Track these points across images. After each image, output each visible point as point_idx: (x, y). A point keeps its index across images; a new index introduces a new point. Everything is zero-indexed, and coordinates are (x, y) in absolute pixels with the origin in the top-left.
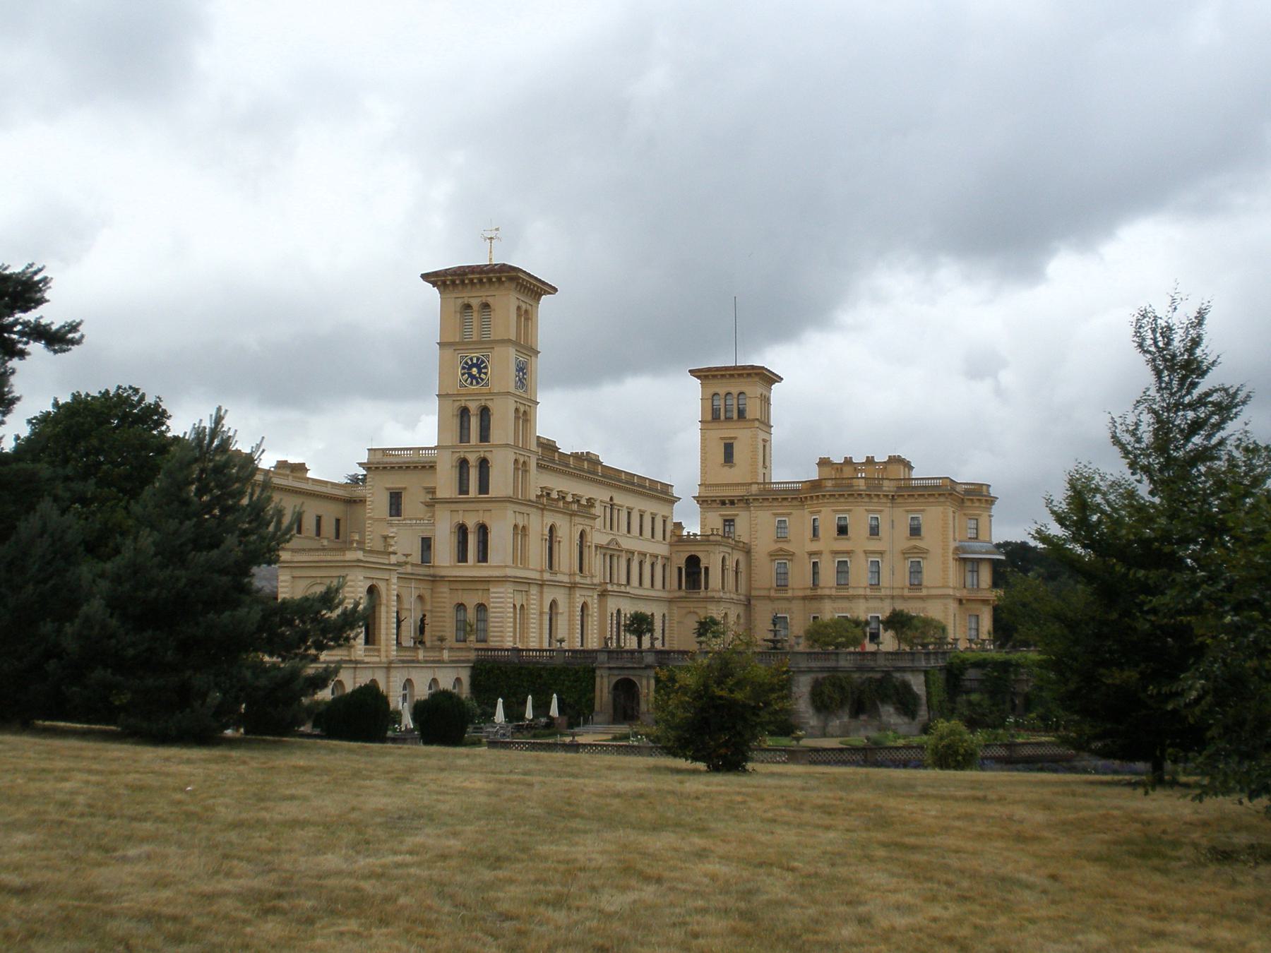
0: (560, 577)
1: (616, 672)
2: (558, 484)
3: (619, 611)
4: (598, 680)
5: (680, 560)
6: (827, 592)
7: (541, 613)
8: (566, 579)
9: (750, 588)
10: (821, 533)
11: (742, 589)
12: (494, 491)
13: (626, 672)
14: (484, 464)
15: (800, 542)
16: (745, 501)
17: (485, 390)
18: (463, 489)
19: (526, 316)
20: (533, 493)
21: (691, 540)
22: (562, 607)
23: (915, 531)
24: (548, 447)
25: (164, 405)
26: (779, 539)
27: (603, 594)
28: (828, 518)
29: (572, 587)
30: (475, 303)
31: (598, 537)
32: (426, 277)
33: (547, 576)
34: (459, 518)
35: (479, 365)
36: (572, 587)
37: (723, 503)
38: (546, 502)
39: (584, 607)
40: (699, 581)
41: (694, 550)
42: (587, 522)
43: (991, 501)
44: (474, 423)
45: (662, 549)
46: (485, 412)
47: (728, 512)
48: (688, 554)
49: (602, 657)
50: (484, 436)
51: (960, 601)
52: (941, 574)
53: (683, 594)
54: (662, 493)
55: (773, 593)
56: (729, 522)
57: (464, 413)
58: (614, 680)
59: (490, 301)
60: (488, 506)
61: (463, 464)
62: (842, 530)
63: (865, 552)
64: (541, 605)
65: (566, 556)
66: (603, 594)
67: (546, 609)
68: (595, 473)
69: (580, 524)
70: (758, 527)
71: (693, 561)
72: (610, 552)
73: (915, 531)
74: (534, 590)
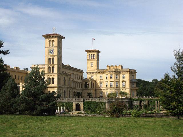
0: (66, 86)
1: (77, 102)
2: (65, 70)
3: (74, 92)
5: (84, 83)
6: (108, 88)
7: (63, 93)
8: (66, 87)
9: (96, 88)
10: (108, 78)
11: (95, 88)
12: (55, 72)
14: (53, 67)
15: (104, 80)
17: (53, 55)
18: (49, 72)
19: (60, 43)
20: (61, 72)
21: (86, 79)
22: (66, 91)
23: (124, 77)
24: (63, 64)
25: (2, 59)
26: (100, 79)
27: (72, 89)
28: (109, 75)
29: (68, 88)
30: (51, 40)
31: (71, 80)
32: (43, 36)
33: (64, 86)
34: (49, 77)
35: (52, 50)
36: (68, 88)
37: (91, 73)
38: (63, 74)
39: (70, 91)
41: (86, 81)
42: (70, 77)
43: (136, 72)
45: (81, 81)
46: (53, 59)
47: (92, 74)
50: (53, 63)
51: (131, 90)
52: (127, 85)
53: (85, 89)
54: (81, 72)
55: (100, 88)
56: (92, 76)
57: (49, 59)
58: (76, 104)
59: (54, 40)
60: (54, 75)
61: (49, 67)
62: (111, 78)
64: (63, 90)
65: (67, 83)
66: (72, 89)
67: (64, 92)
68: (70, 68)
69: (69, 77)
70: (96, 77)
71: (86, 83)
72: (73, 82)
73: (124, 77)
74: (62, 89)
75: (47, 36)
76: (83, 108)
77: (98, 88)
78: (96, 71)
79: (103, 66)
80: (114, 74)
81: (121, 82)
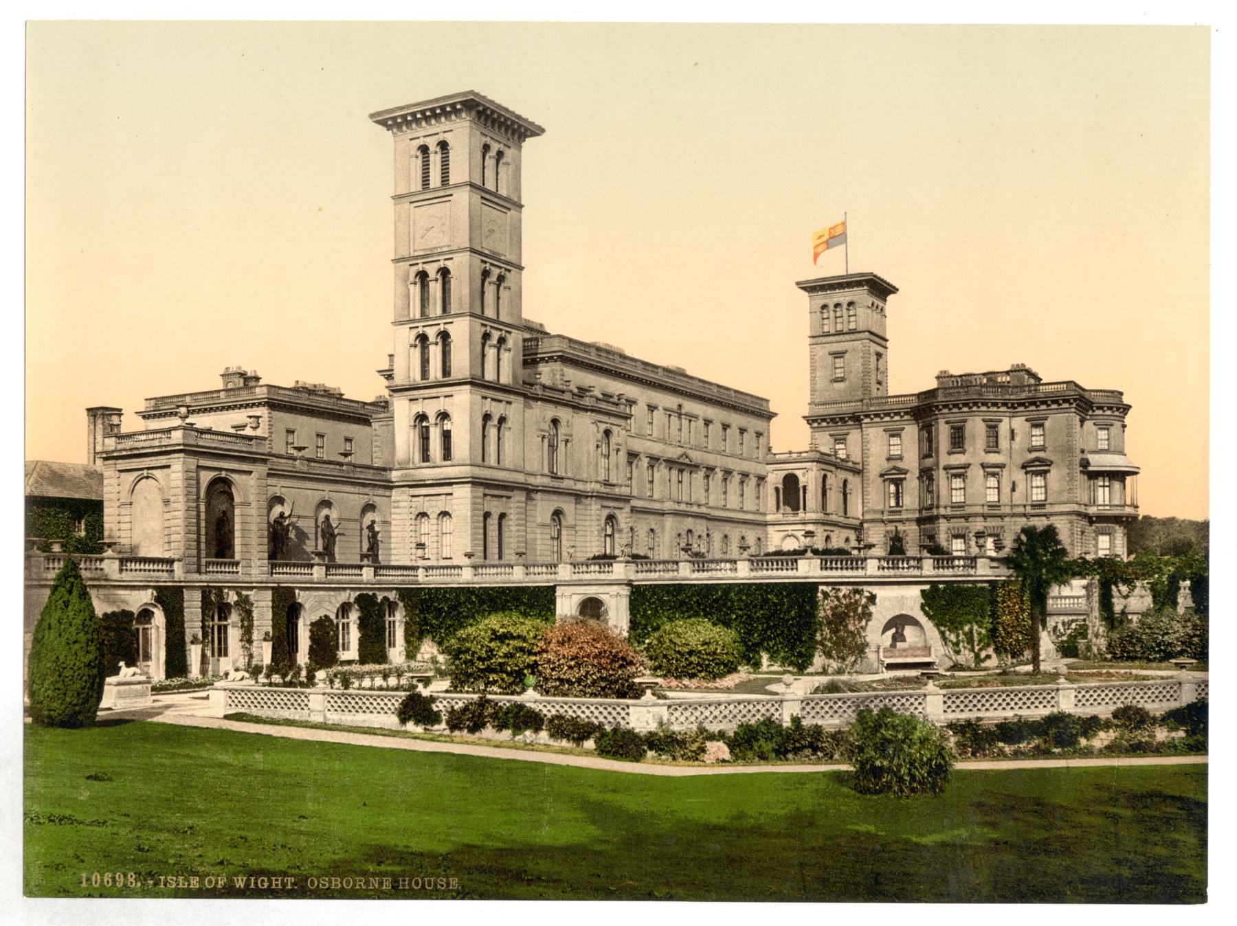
6: (942, 511)
34: (418, 408)
40: (798, 503)
44: (435, 288)
63: (983, 466)
71: (791, 482)
75: (394, 121)
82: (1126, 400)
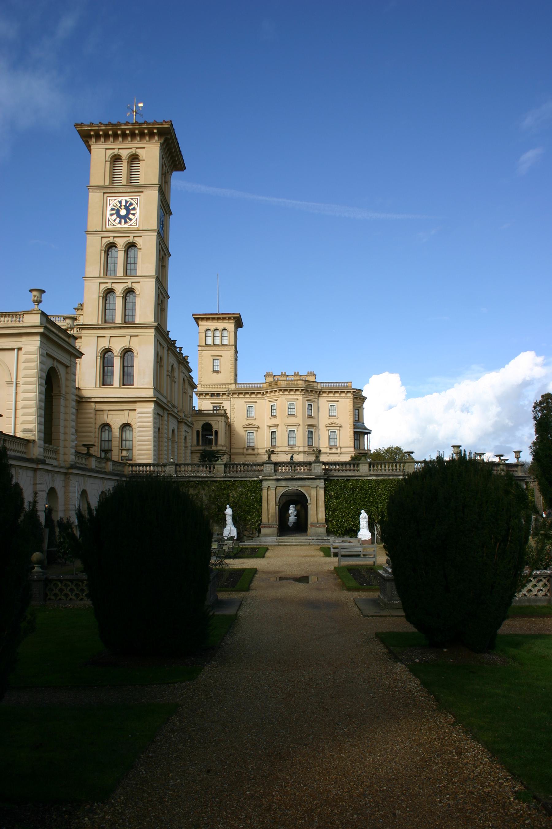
1: (283, 483)
4: (265, 491)
5: (198, 426)
13: (295, 483)
16: (228, 394)
26: (248, 418)
37: (212, 395)
41: (207, 420)
48: (203, 422)
49: (269, 469)
55: (245, 451)
58: (281, 491)
71: (207, 428)
76: (322, 516)
77: (241, 451)
78: (233, 387)
79: (251, 375)
80: (301, 399)
81: (325, 428)
82: (364, 394)
